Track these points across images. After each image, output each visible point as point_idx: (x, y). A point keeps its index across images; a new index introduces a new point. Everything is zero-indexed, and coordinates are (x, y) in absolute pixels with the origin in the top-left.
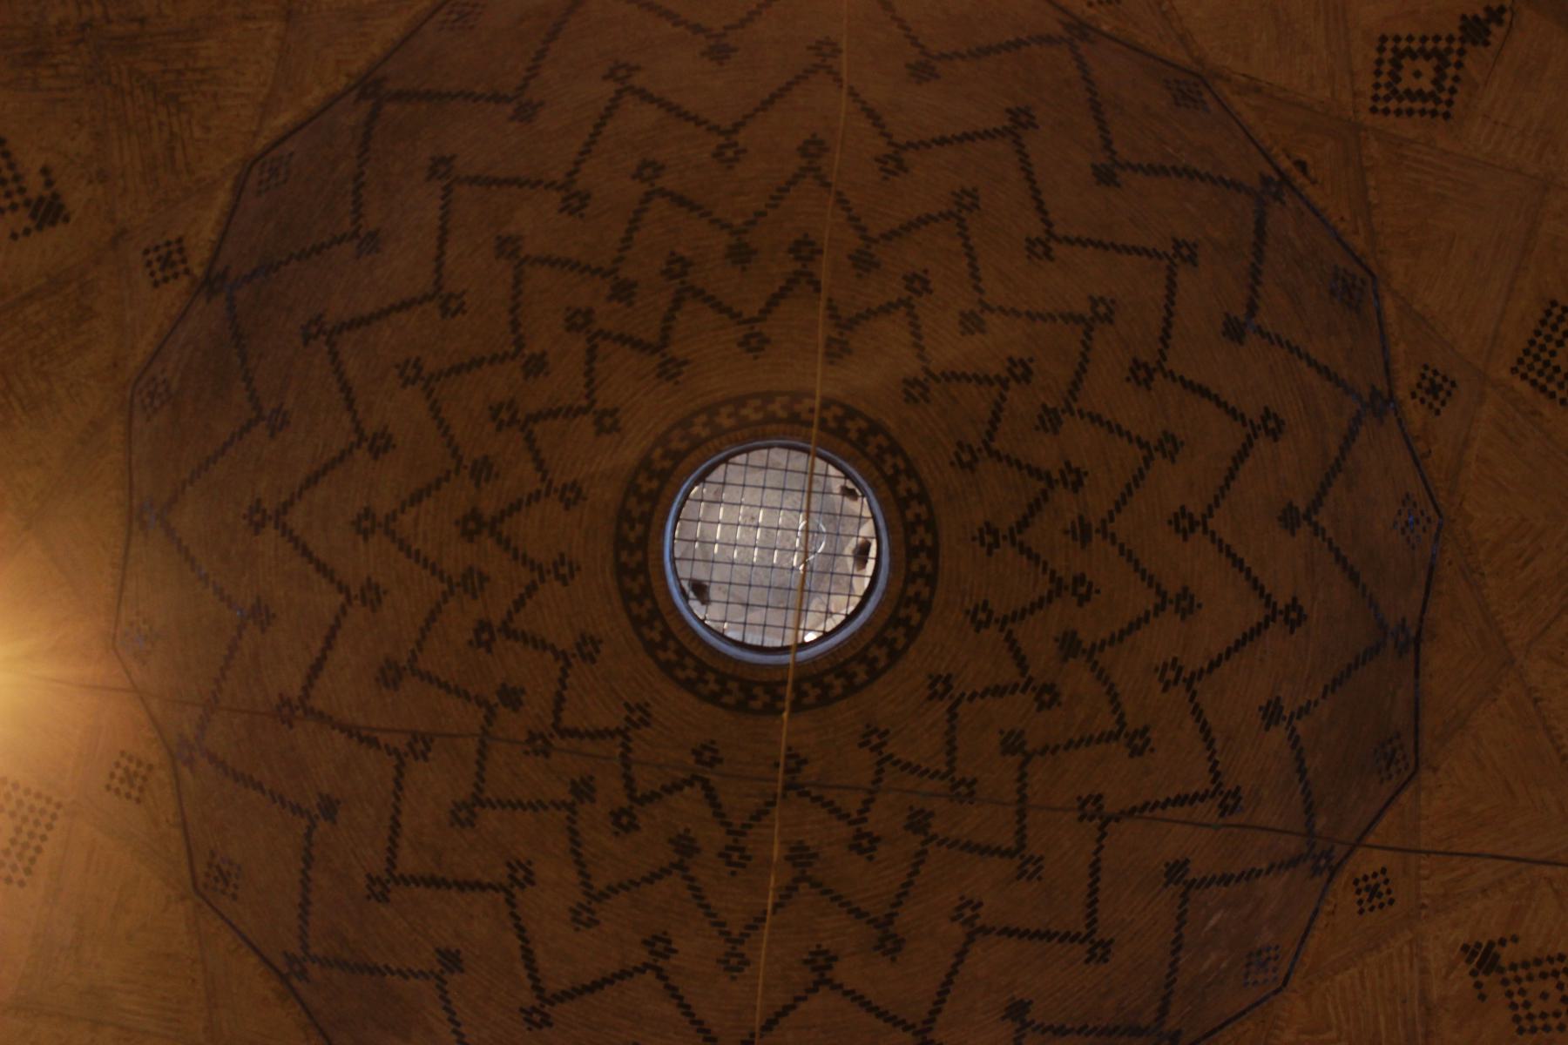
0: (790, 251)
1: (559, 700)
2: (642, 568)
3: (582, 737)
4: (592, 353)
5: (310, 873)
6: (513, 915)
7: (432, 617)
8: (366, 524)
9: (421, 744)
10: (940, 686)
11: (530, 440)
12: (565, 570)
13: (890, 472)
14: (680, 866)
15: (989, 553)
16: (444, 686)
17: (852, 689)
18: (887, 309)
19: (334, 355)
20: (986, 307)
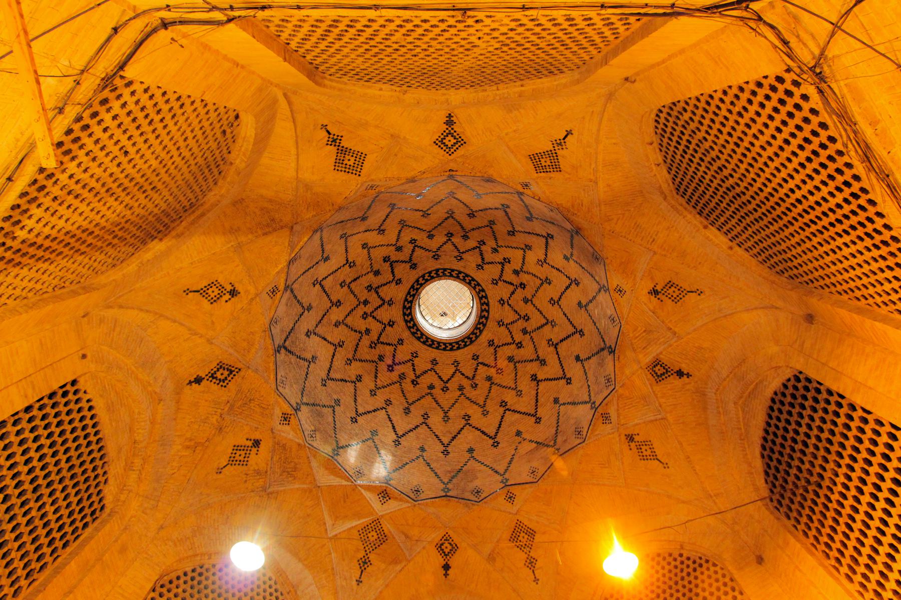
1: (440, 377)
2: (427, 338)
4: (374, 317)
7: (403, 391)
8: (373, 393)
9: (426, 416)
10: (502, 302)
11: (382, 343)
12: (415, 355)
17: (487, 318)
18: (413, 251)
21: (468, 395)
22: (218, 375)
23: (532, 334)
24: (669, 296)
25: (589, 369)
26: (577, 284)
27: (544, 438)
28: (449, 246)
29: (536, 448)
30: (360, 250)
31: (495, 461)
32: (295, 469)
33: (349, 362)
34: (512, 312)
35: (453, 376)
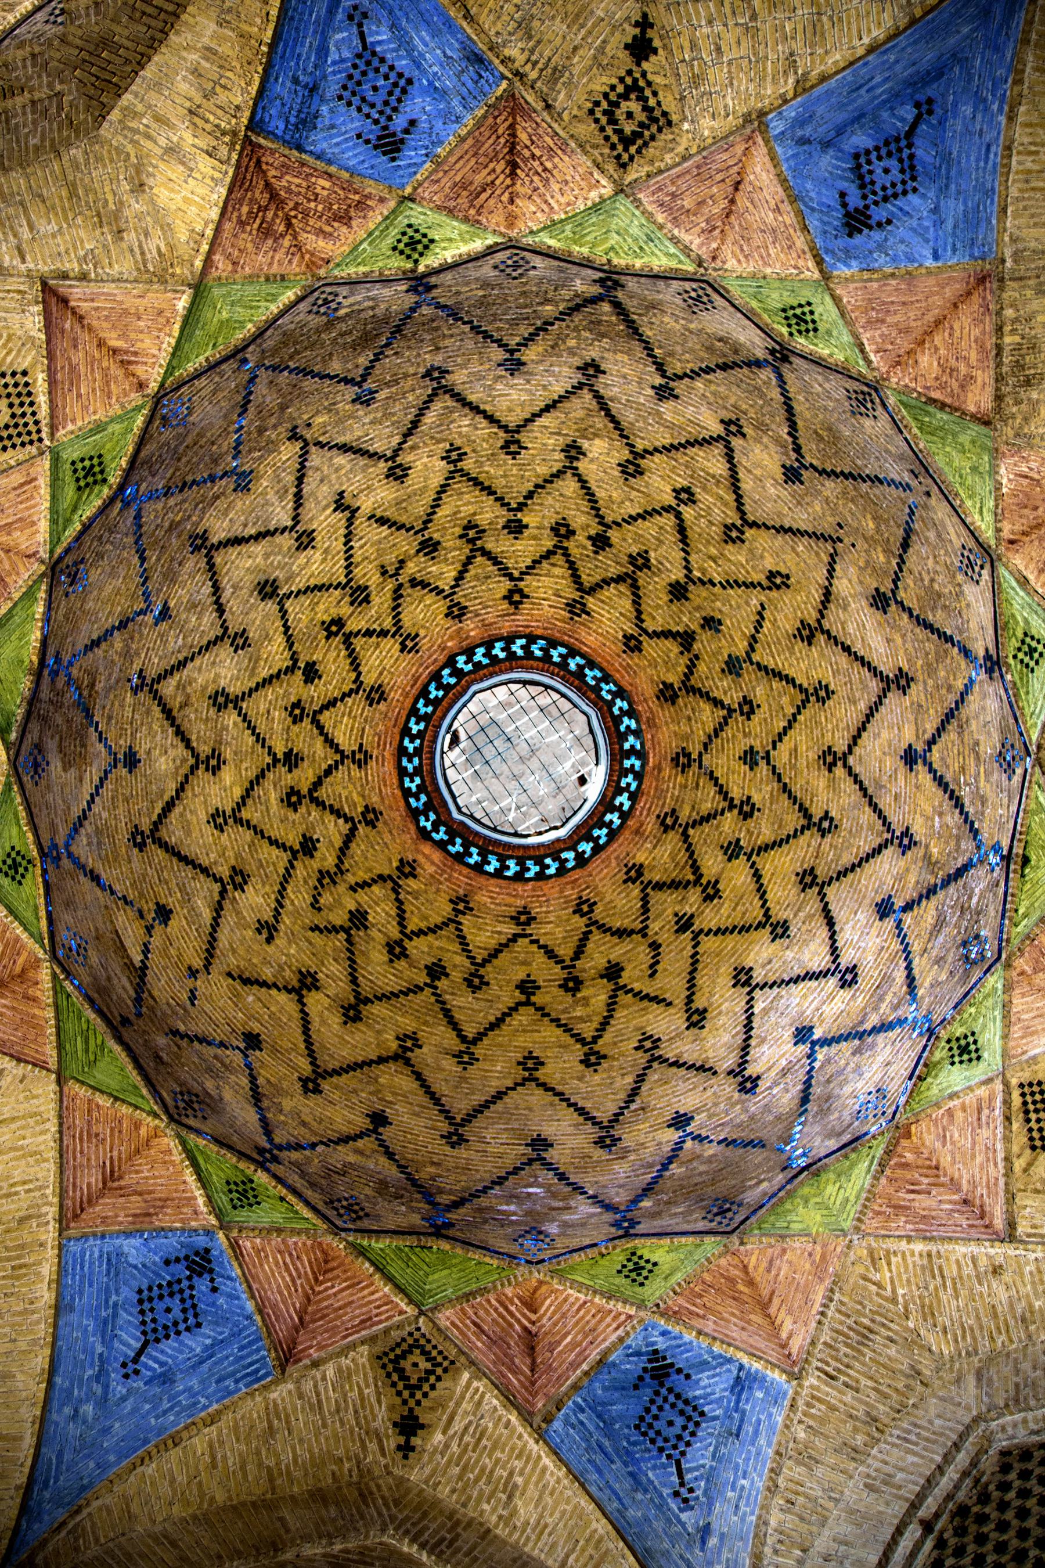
0: (704, 618)
1: (332, 703)
3: (321, 733)
4: (549, 554)
5: (116, 633)
6: (186, 776)
7: (319, 588)
11: (469, 561)
13: (623, 784)
14: (294, 854)
15: (625, 882)
16: (287, 628)
18: (717, 703)
19: (430, 399)
20: (767, 757)
21: (270, 775)
22: (633, 105)
23: (428, 991)
24: (654, 1410)
25: (360, 1152)
26: (600, 1142)
27: (156, 993)
28: (708, 800)
30: (769, 563)
31: (98, 832)
32: (266, 232)
33: (454, 456)
34: (493, 943)
35: (329, 742)
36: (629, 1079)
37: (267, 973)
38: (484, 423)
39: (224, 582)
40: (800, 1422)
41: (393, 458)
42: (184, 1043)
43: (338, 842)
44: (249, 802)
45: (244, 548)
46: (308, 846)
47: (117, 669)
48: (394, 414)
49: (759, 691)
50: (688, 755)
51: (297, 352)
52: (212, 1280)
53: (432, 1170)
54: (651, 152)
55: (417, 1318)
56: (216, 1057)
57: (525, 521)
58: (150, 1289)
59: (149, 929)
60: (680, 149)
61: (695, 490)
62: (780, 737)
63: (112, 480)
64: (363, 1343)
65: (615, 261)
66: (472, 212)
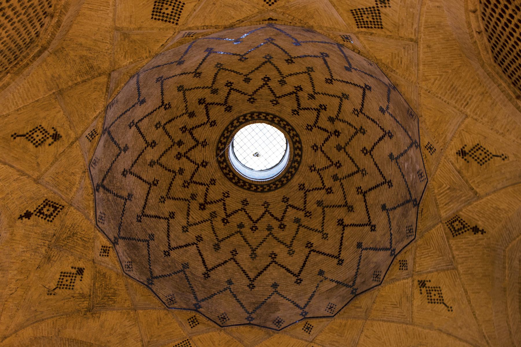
0: (199, 104)
1: (250, 217)
2: (239, 179)
3: (260, 219)
4: (188, 158)
5: (238, 298)
6: (279, 265)
7: (213, 229)
8: (185, 229)
9: (234, 253)
10: (315, 148)
11: (195, 183)
12: (226, 195)
13: (264, 118)
14: (300, 225)
15: (299, 115)
16: (228, 237)
17: (299, 163)
18: (229, 94)
19: (147, 216)
20: (246, 75)
21: (275, 235)
22: (45, 210)
23: (342, 181)
24: (476, 158)
25: (394, 218)
26: (391, 137)
27: (345, 279)
28: (265, 91)
29: (336, 287)
30: (176, 93)
31: (297, 297)
32: (114, 294)
33: (163, 200)
34: (325, 159)
35: (262, 216)
36: (369, 121)
37: (339, 236)
38: (150, 195)
39: (217, 263)
40: (482, 119)
41: (168, 219)
42: (359, 271)
43: (295, 210)
44: (285, 242)
45: (205, 259)
46: (297, 221)
47: (248, 295)
48: (154, 225)
49: (222, 82)
50: (250, 99)
51: (144, 267)
52: (427, 281)
53: (399, 196)
54: (57, 202)
55: (442, 223)
56: (364, 260)
57: (178, 169)
58: (428, 299)
59: (326, 279)
60: (53, 195)
61: (155, 123)
62: (237, 73)
63: (194, 314)
64: (448, 242)
65: (91, 192)
66: (91, 241)
